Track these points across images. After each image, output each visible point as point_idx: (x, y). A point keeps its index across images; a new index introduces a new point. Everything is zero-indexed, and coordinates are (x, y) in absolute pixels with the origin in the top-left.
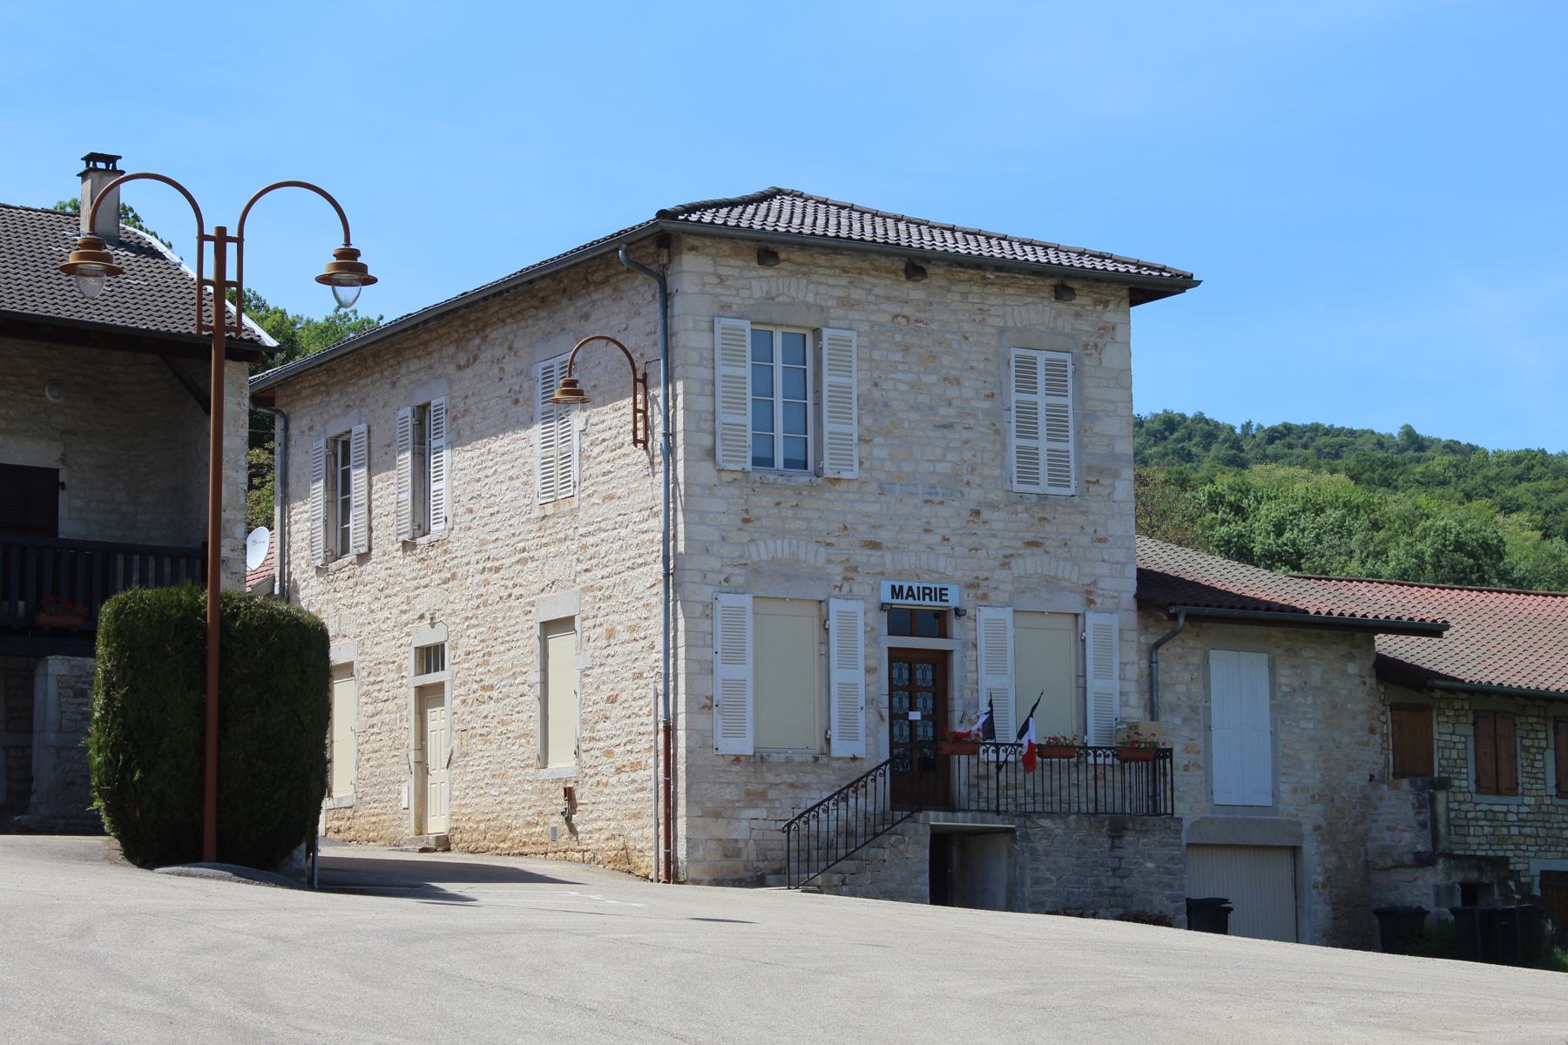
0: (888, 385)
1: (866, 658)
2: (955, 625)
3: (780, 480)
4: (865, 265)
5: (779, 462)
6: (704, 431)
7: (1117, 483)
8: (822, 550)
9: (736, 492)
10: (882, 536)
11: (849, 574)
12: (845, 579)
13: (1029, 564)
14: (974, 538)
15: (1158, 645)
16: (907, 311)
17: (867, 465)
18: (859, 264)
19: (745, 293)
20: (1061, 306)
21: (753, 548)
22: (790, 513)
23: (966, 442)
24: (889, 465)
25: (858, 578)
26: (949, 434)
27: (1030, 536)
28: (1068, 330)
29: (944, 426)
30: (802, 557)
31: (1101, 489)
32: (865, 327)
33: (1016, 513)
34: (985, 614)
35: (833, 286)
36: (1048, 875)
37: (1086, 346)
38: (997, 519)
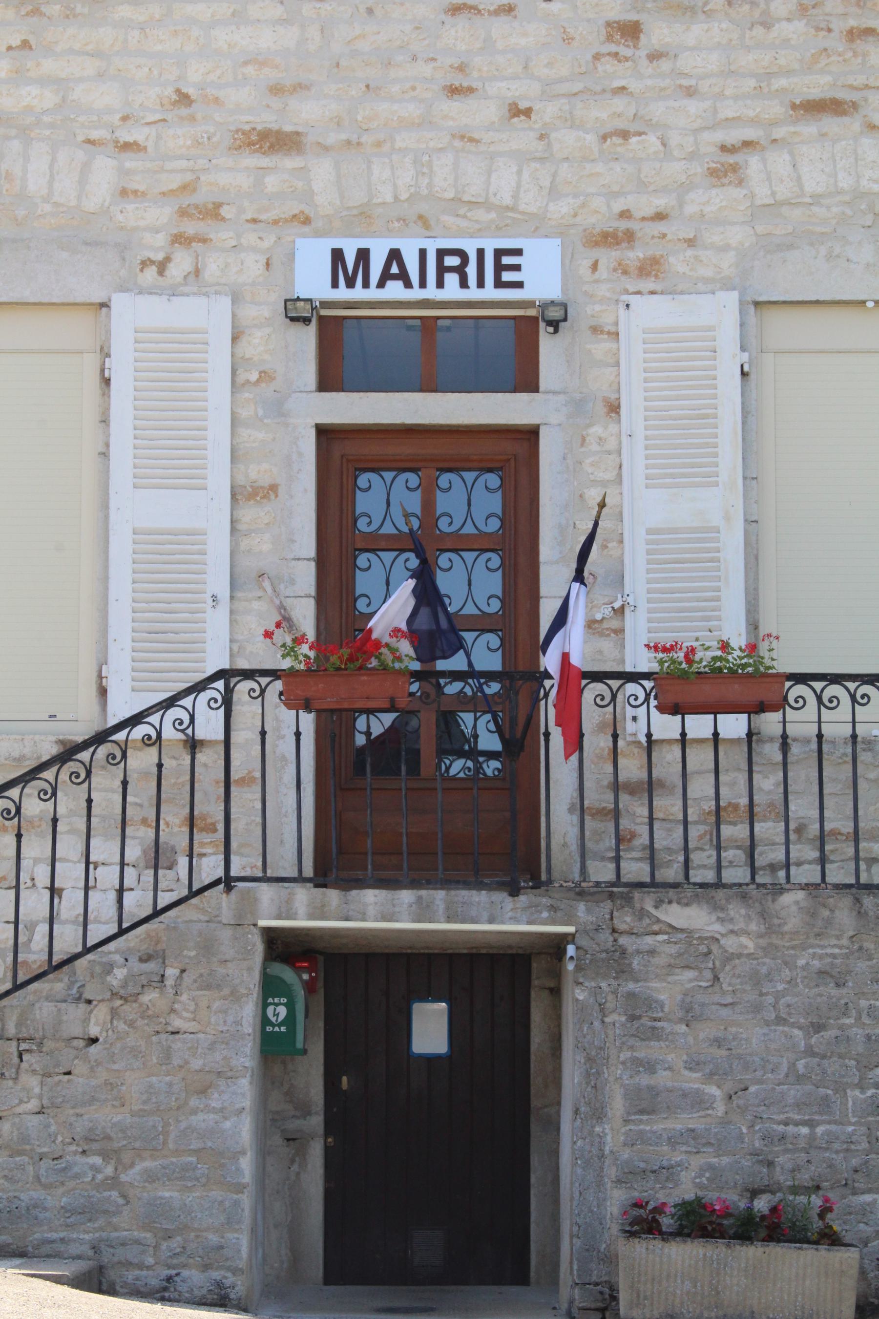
1: (235, 457)
2: (550, 349)
8: (105, 172)
10: (305, 113)
11: (190, 228)
14: (619, 104)
25: (222, 235)
27: (817, 86)
30: (36, 184)
34: (648, 315)
36: (692, 1081)
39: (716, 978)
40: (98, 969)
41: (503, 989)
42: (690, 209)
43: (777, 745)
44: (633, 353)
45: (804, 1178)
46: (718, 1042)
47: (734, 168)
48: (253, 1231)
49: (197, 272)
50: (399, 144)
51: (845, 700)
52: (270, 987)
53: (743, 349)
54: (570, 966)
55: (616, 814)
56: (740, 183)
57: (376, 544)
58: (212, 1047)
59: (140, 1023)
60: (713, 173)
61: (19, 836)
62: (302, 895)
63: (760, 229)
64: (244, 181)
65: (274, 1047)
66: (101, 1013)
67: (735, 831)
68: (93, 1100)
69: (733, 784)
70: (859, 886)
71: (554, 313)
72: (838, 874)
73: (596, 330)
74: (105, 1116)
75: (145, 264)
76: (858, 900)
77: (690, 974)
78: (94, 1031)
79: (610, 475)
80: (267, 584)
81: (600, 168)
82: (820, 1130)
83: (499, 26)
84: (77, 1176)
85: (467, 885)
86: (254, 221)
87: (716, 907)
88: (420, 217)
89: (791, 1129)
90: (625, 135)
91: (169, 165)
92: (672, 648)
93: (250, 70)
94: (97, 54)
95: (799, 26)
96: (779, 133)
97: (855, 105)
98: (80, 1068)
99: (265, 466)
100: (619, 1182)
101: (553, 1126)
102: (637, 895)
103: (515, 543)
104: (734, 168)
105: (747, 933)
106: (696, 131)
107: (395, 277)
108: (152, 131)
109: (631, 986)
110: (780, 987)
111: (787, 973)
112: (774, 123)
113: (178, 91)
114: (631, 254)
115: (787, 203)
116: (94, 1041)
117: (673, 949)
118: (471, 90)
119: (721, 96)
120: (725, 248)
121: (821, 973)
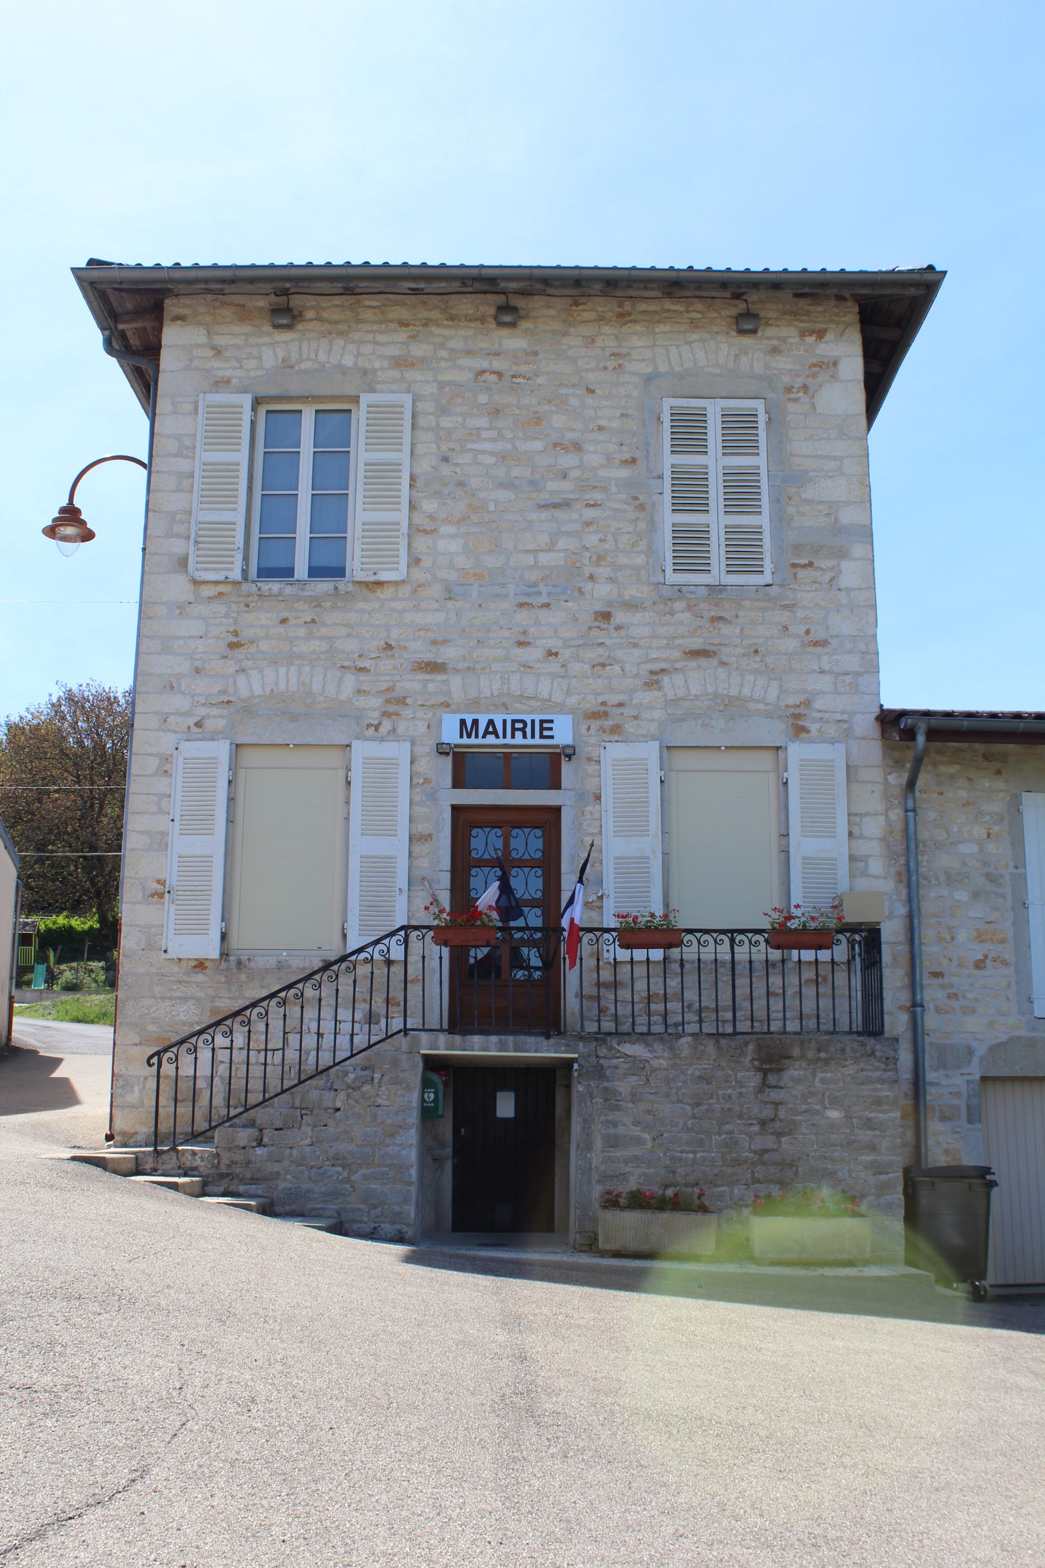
0: (467, 458)
1: (411, 820)
2: (566, 768)
3: (288, 590)
4: (435, 314)
5: (301, 569)
6: (179, 536)
7: (845, 565)
8: (350, 681)
9: (220, 608)
10: (448, 654)
11: (391, 708)
12: (386, 714)
13: (695, 681)
14: (600, 650)
15: (911, 785)
16: (497, 364)
17: (427, 562)
18: (426, 314)
19: (252, 364)
20: (747, 341)
21: (242, 680)
22: (301, 632)
23: (588, 524)
24: (461, 561)
25: (407, 712)
26: (561, 515)
27: (696, 643)
28: (759, 369)
29: (555, 506)
30: (316, 687)
31: (817, 574)
32: (430, 389)
33: (672, 614)
34: (614, 752)
35: (384, 345)
36: (636, 1131)
37: (789, 389)
38: (639, 624)
39: (648, 1080)
40: (340, 1074)
41: (542, 1085)
42: (635, 701)
43: (678, 964)
44: (607, 770)
45: (691, 1179)
46: (649, 1112)
47: (657, 682)
48: (417, 1205)
49: (394, 730)
50: (493, 669)
51: (711, 942)
52: (426, 1084)
53: (661, 769)
54: (576, 1074)
55: (598, 998)
56: (660, 689)
57: (480, 863)
58: (397, 1113)
59: (361, 1101)
60: (646, 684)
61: (302, 1007)
62: (442, 1038)
63: (669, 711)
64: (418, 686)
65: (428, 1115)
66: (342, 1095)
67: (657, 1007)
68: (337, 1139)
69: (657, 983)
70: (718, 1034)
71: (569, 751)
72: (708, 1028)
73: (589, 759)
74: (344, 1147)
75: (369, 726)
76: (717, 1041)
77: (635, 1078)
78: (338, 1105)
79: (596, 831)
80: (426, 883)
81: (591, 681)
82: (699, 1155)
83: (543, 614)
84: (329, 1177)
85: (525, 1034)
86: (423, 705)
87: (648, 1045)
88: (504, 704)
89: (684, 1155)
90: (604, 665)
91: (381, 679)
92: (627, 916)
93: (422, 633)
94: (347, 625)
95: (688, 615)
96: (678, 665)
97: (714, 653)
98: (331, 1123)
99: (426, 825)
100: (599, 1181)
101: (567, 1154)
102: (609, 1039)
103: (549, 863)
104: (657, 682)
105: (663, 1057)
106: (638, 664)
107: (491, 733)
108: (373, 662)
109: (606, 1084)
110: (679, 1084)
111: (682, 1077)
112: (676, 661)
113: (386, 643)
114: (607, 723)
115: (683, 699)
116: (338, 1110)
117: (626, 1066)
118: (529, 643)
119: (650, 647)
120: (652, 720)
121: (700, 1077)
